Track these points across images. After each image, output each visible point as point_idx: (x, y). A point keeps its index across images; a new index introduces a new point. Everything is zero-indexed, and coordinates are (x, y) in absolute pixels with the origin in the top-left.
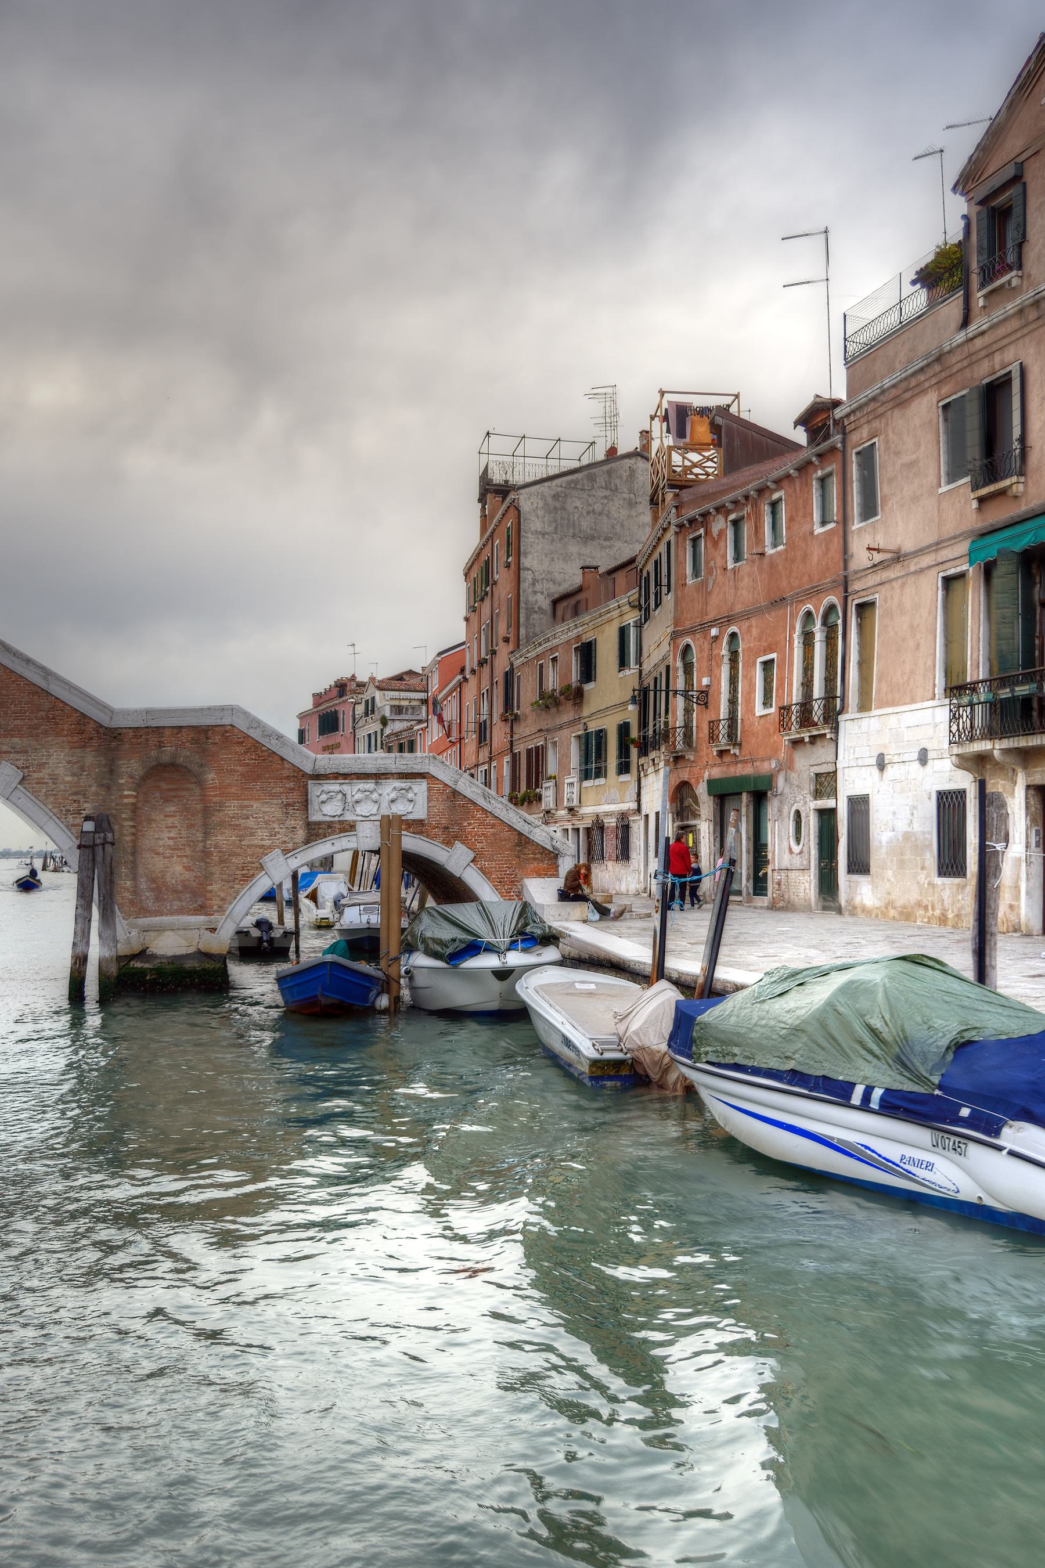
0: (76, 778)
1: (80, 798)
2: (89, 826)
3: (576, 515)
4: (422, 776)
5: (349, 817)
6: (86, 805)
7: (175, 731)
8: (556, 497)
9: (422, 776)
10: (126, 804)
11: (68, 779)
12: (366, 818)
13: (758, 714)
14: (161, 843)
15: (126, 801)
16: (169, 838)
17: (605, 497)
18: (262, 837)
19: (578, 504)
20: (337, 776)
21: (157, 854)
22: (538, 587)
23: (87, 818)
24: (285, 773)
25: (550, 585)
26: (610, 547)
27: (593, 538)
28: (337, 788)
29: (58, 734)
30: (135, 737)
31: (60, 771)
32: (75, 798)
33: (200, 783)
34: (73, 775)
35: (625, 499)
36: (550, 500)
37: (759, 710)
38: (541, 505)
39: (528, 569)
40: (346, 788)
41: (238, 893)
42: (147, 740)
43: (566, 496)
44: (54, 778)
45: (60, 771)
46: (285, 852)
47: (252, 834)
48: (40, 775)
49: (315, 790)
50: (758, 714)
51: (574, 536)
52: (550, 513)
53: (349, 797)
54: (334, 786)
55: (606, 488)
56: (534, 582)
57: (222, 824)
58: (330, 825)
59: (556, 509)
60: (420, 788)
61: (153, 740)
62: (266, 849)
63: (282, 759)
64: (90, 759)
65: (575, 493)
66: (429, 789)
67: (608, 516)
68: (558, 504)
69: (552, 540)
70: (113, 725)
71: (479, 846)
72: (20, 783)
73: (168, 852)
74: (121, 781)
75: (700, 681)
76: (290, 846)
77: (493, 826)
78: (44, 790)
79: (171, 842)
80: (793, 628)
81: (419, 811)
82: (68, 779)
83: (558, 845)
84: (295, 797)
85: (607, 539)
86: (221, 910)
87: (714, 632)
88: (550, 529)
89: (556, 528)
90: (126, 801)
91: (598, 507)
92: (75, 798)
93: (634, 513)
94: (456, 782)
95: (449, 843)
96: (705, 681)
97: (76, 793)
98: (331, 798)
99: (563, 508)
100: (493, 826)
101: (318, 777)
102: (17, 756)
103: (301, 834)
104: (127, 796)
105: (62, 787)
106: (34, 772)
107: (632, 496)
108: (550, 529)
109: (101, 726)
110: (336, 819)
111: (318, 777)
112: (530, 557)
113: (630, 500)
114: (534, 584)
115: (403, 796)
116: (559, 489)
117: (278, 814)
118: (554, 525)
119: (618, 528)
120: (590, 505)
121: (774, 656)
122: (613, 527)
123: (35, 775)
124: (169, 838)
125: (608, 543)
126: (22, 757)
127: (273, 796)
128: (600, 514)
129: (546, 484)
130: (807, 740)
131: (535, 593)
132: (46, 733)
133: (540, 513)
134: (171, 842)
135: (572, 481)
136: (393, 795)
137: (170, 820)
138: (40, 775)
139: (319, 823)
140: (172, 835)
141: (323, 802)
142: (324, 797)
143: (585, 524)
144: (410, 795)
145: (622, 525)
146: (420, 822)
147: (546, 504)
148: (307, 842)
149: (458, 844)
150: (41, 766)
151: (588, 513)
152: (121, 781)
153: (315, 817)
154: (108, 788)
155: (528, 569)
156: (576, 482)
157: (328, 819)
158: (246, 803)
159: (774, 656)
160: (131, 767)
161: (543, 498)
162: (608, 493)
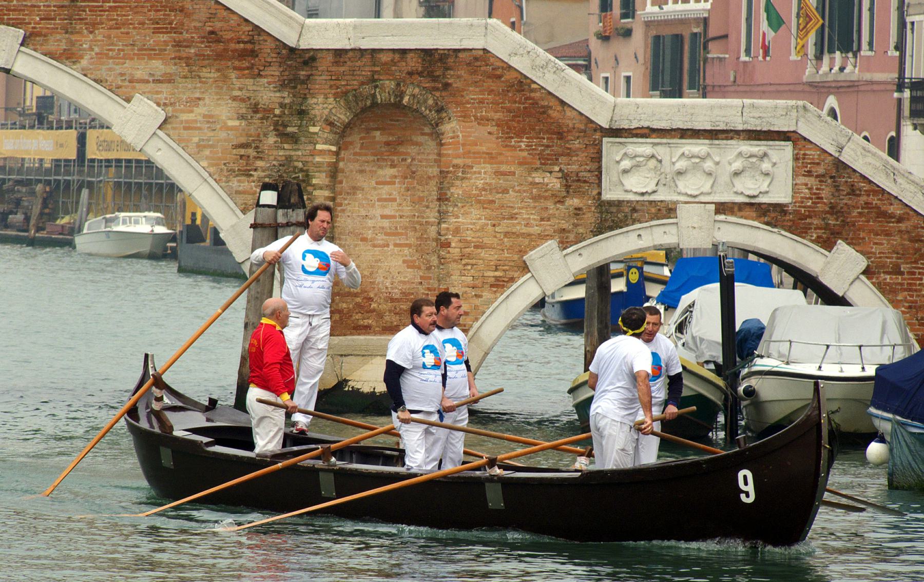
0: (244, 123)
1: (251, 152)
2: (269, 197)
4: (784, 136)
5: (663, 195)
6: (259, 163)
9: (784, 136)
12: (693, 199)
14: (370, 223)
15: (318, 159)
16: (383, 217)
21: (364, 240)
23: (266, 187)
30: (336, 63)
33: (437, 136)
34: (242, 117)
40: (662, 152)
47: (512, 217)
48: (191, 116)
49: (611, 150)
54: (643, 148)
60: (783, 153)
63: (563, 103)
70: (303, 45)
72: (160, 128)
73: (381, 238)
74: (313, 129)
78: (196, 140)
79: (386, 223)
90: (318, 159)
94: (841, 149)
95: (827, 244)
98: (637, 166)
101: (615, 133)
103: (590, 218)
104: (322, 152)
106: (182, 111)
109: (285, 46)
111: (615, 133)
115: (753, 167)
123: (184, 117)
124: (383, 217)
126: (165, 88)
134: (386, 223)
136: (737, 165)
137: (385, 190)
138: (191, 116)
139: (619, 203)
140: (387, 212)
141: (625, 172)
142: (626, 164)
144: (766, 166)
146: (779, 208)
148: (599, 230)
149: (841, 245)
152: (313, 129)
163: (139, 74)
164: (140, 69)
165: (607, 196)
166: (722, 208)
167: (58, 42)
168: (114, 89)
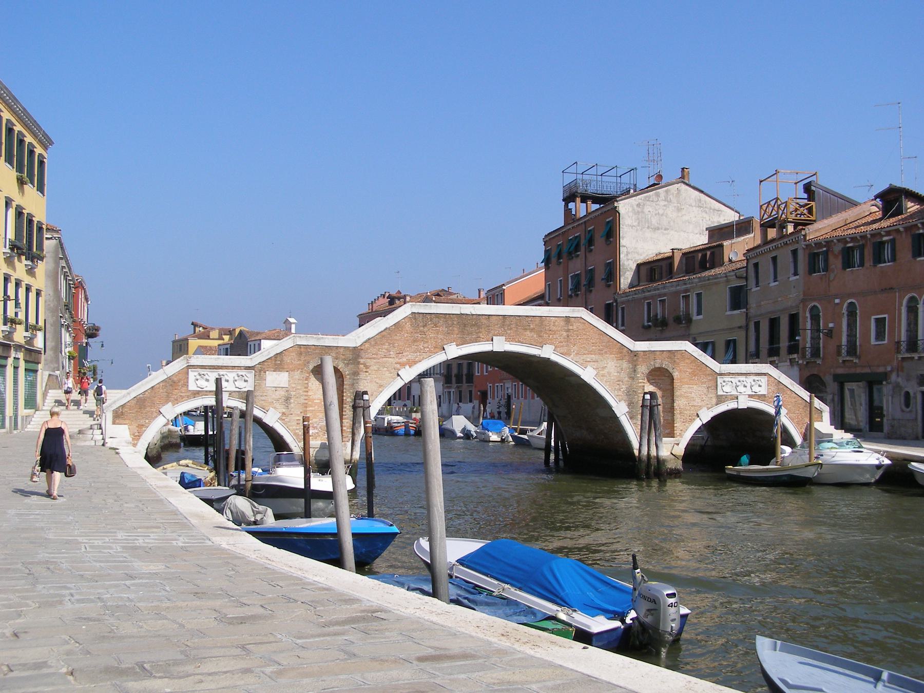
3: (649, 216)
6: (623, 386)
7: (661, 353)
8: (638, 205)
9: (765, 374)
10: (640, 386)
11: (616, 374)
13: (872, 343)
15: (640, 384)
17: (665, 206)
18: (698, 402)
19: (650, 210)
20: (729, 374)
22: (630, 256)
24: (708, 373)
25: (636, 255)
26: (668, 234)
27: (658, 229)
28: (730, 380)
29: (611, 354)
30: (644, 355)
31: (612, 371)
32: (618, 383)
35: (675, 207)
36: (635, 207)
37: (873, 341)
38: (631, 210)
39: (624, 246)
40: (732, 380)
41: (688, 428)
42: (649, 357)
43: (644, 205)
44: (609, 373)
45: (612, 371)
46: (708, 409)
49: (720, 380)
50: (872, 343)
51: (648, 227)
52: (635, 214)
53: (734, 383)
54: (727, 379)
55: (665, 200)
56: (628, 253)
57: (681, 395)
58: (726, 396)
59: (638, 212)
60: (764, 380)
61: (652, 356)
62: (701, 407)
64: (625, 365)
65: (648, 203)
66: (768, 381)
67: (666, 217)
68: (639, 209)
69: (637, 230)
71: (789, 407)
75: (826, 324)
76: (710, 406)
77: (795, 398)
80: (901, 305)
81: (763, 391)
82: (616, 374)
83: (822, 407)
84: (712, 383)
85: (666, 229)
86: (681, 435)
87: (837, 301)
88: (635, 224)
89: (639, 223)
90: (640, 384)
91: (661, 212)
92: (618, 383)
93: (680, 215)
94: (779, 377)
96: (831, 325)
97: (619, 381)
98: (727, 384)
99: (643, 212)
100: (795, 398)
101: (721, 374)
102: (593, 363)
103: (714, 401)
105: (613, 378)
107: (679, 205)
108: (635, 224)
110: (729, 394)
111: (721, 374)
112: (625, 239)
113: (678, 207)
114: (627, 255)
116: (640, 201)
117: (705, 390)
118: (637, 221)
119: (672, 223)
120: (656, 210)
121: (886, 316)
122: (669, 222)
123: (601, 372)
125: (666, 232)
126: (596, 364)
127: (702, 383)
128: (662, 215)
129: (633, 198)
130: (917, 358)
131: (628, 260)
132: (606, 353)
133: (631, 214)
135: (647, 197)
139: (722, 395)
143: (654, 221)
145: (674, 222)
147: (634, 209)
150: (604, 368)
151: (656, 215)
153: (720, 393)
154: (633, 378)
155: (624, 246)
156: (649, 197)
157: (725, 394)
158: (691, 386)
159: (886, 316)
160: (643, 369)
161: (632, 206)
162: (666, 203)
163: (588, 360)
164: (589, 358)
165: (719, 393)
166: (750, 396)
167: (564, 350)
168: (582, 364)
